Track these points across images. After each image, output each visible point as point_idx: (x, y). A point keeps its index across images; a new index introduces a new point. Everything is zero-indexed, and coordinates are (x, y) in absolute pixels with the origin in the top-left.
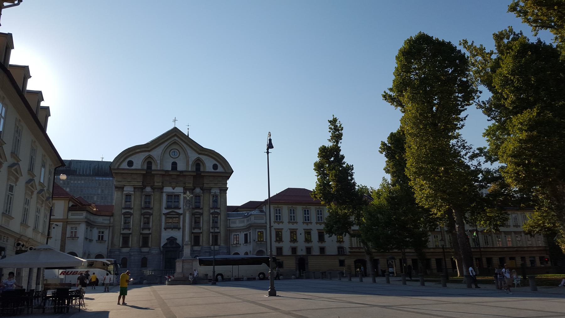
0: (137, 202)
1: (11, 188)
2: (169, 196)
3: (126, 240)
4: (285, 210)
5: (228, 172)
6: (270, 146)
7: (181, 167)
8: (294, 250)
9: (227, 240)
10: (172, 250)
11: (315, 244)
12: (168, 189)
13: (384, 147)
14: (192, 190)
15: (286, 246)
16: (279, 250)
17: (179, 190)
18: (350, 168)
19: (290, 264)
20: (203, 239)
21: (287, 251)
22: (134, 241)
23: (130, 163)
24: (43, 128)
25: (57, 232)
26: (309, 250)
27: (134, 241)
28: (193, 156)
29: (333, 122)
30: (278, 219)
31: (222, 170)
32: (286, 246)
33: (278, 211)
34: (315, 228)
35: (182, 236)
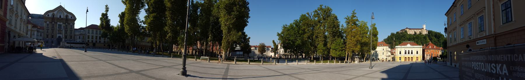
0: (50, 26)
1: (16, 20)
2: (59, 25)
3: (47, 36)
4: (91, 30)
5: (75, 19)
6: (87, 11)
7: (62, 17)
8: (92, 41)
9: (74, 38)
10: (59, 40)
11: (98, 40)
12: (58, 23)
13: (120, 16)
14: (65, 24)
15: (90, 40)
16: (88, 41)
17: (61, 23)
18: (110, 20)
19: (91, 45)
20: (68, 37)
21: (90, 41)
22: (50, 36)
23: (48, 15)
24: (24, 4)
25: (29, 33)
26: (96, 41)
27: (50, 36)
28: (66, 14)
29: (107, 6)
30: (89, 33)
31: (74, 18)
32: (90, 40)
33: (89, 31)
34: (99, 36)
35: (62, 36)
